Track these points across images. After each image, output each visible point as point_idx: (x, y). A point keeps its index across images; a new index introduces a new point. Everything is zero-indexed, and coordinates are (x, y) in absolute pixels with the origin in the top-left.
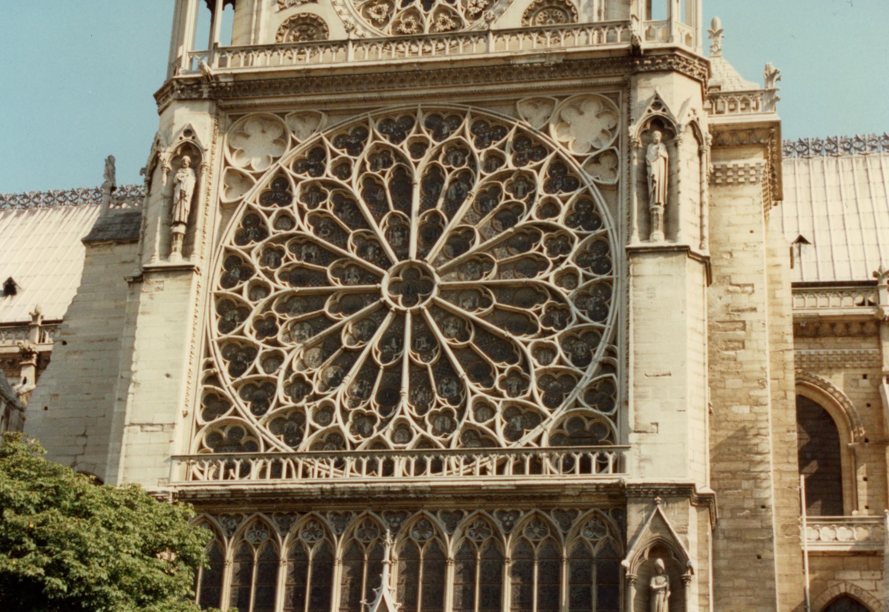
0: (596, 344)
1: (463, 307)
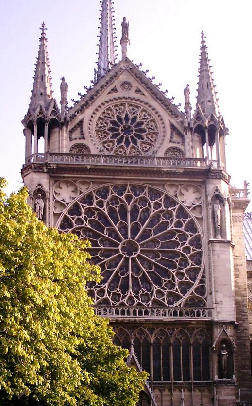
0: (198, 273)
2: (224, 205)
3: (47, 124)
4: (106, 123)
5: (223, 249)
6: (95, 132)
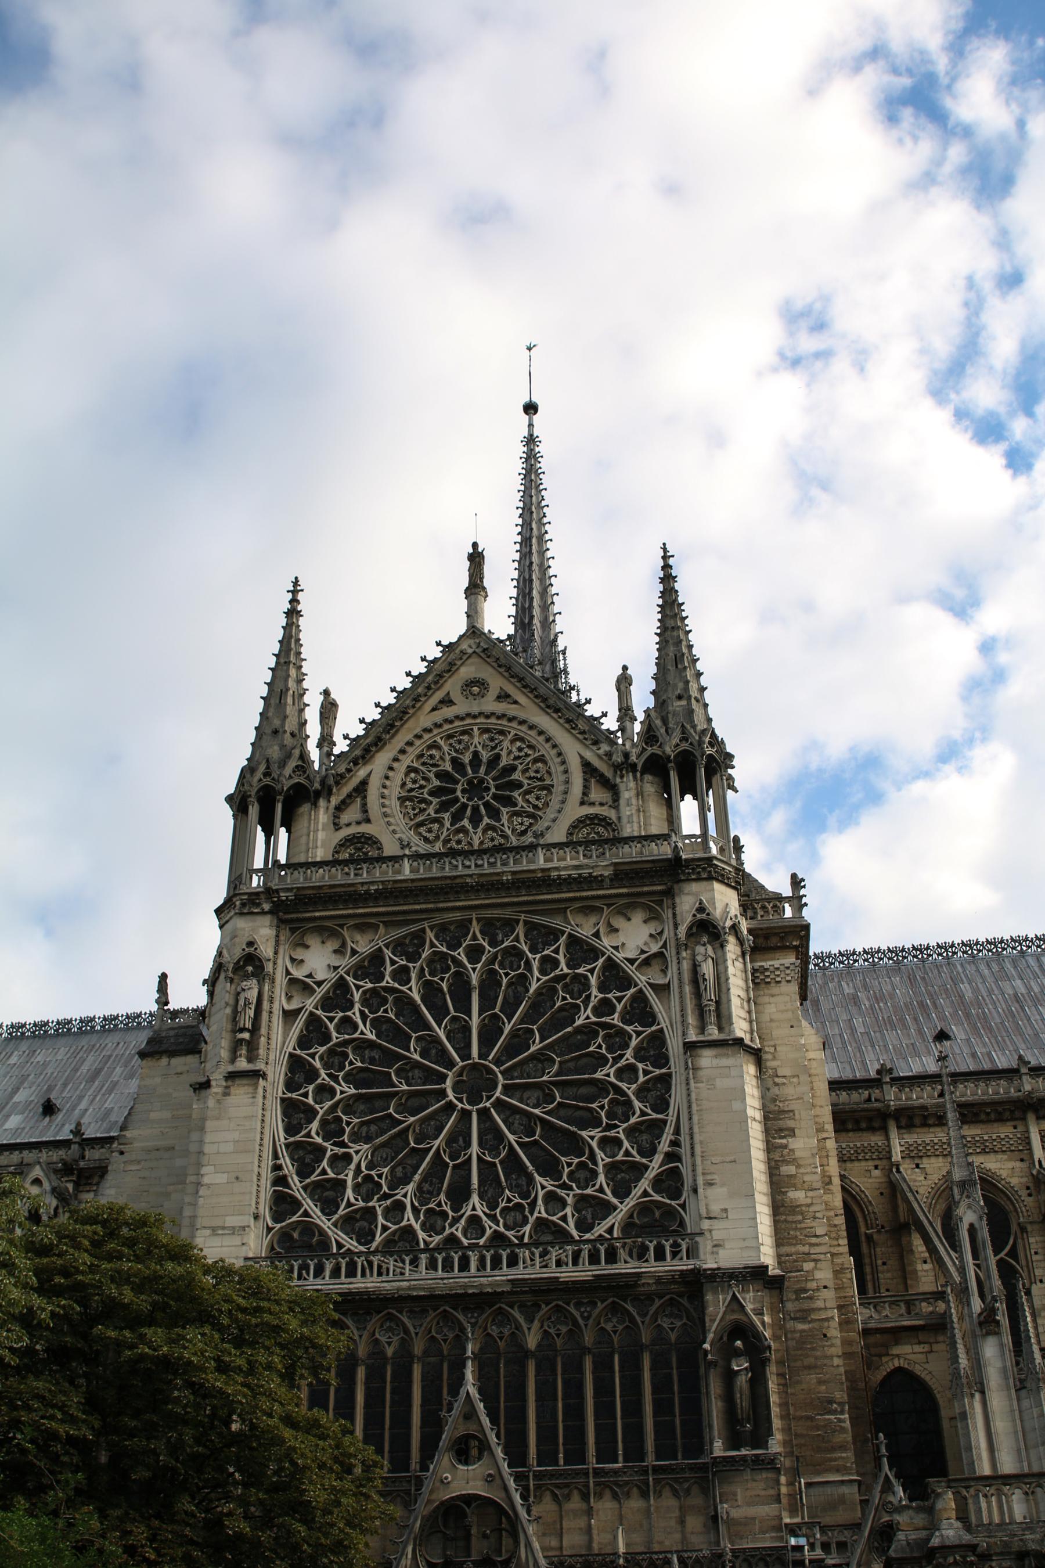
0: (660, 1136)
1: (527, 1105)
2: (722, 946)
3: (281, 798)
4: (424, 778)
5: (724, 1062)
6: (398, 803)
